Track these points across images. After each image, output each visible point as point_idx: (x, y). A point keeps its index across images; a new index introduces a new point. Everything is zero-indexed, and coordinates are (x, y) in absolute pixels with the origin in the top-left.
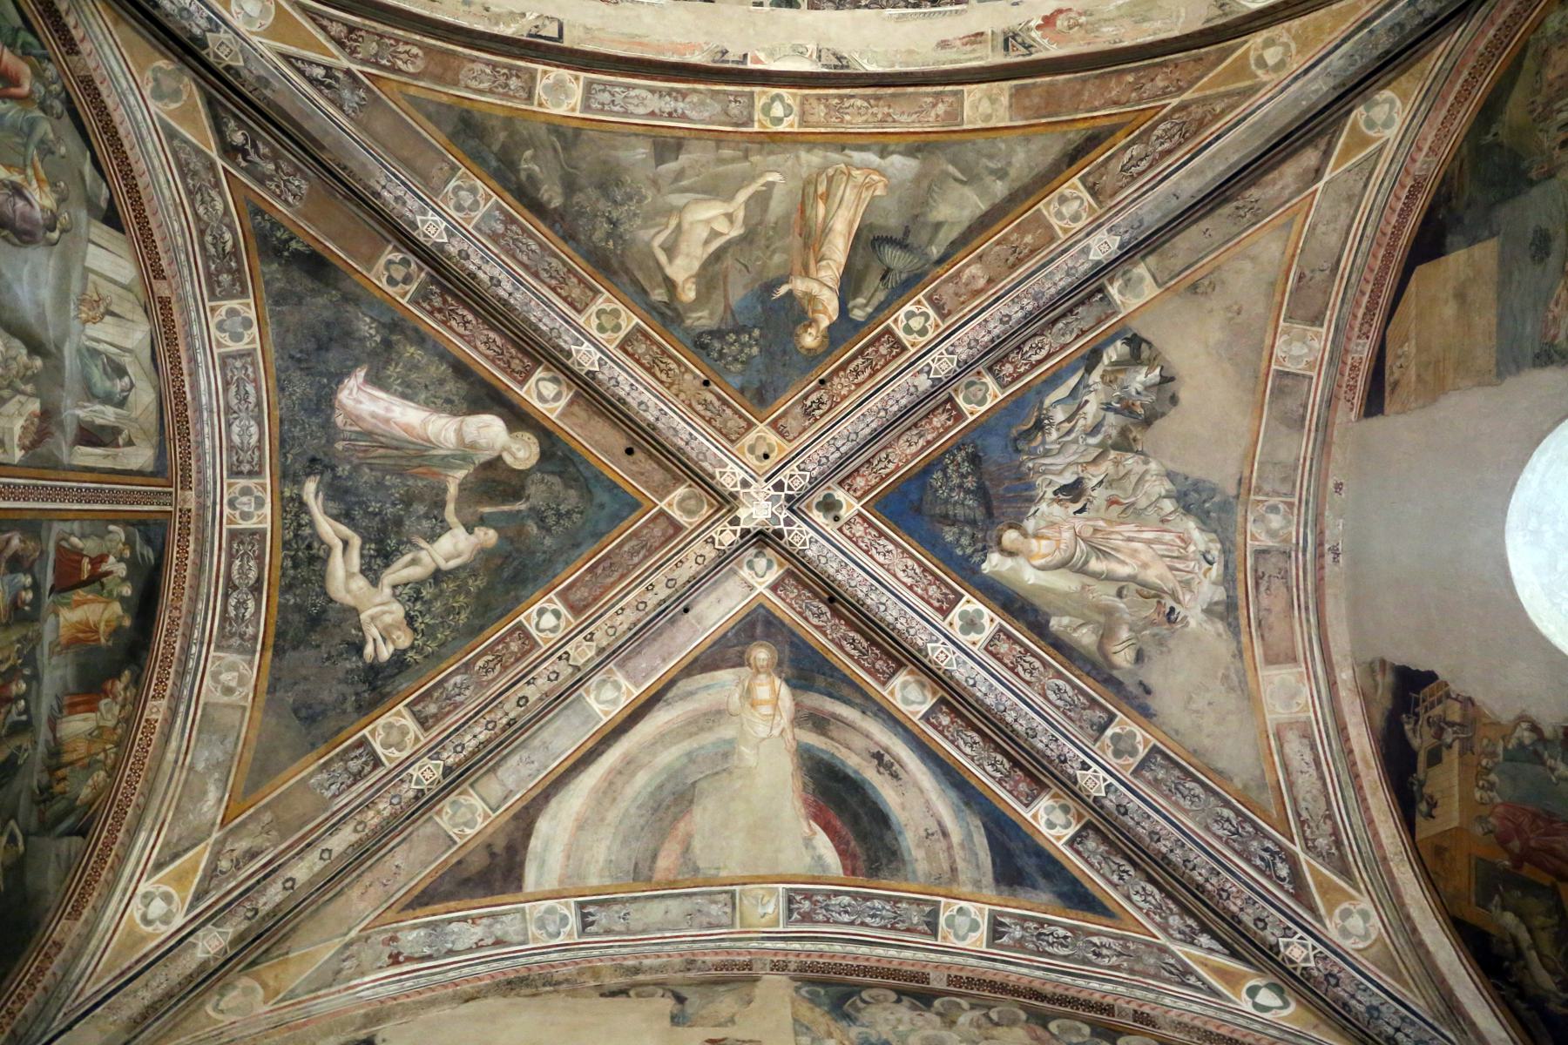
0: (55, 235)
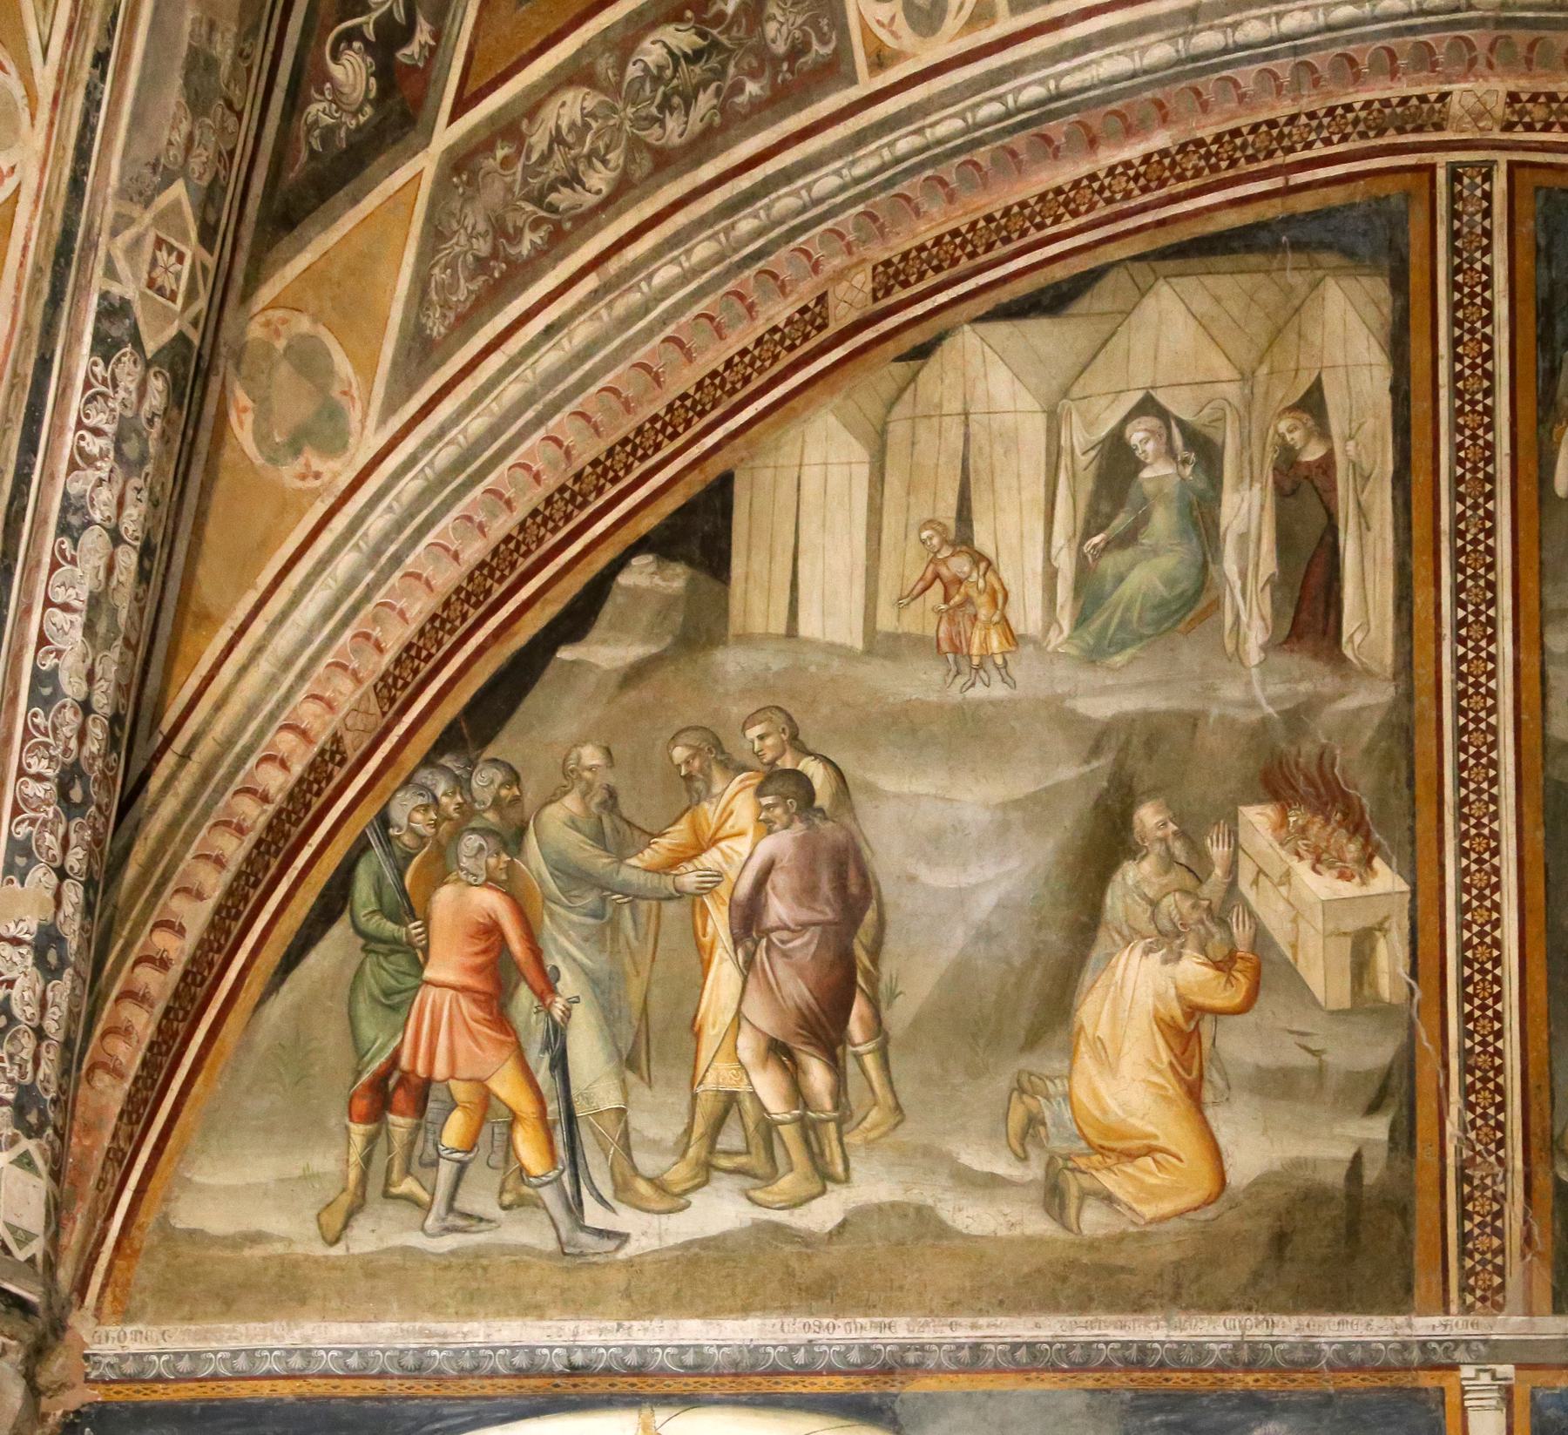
0: (815, 771)
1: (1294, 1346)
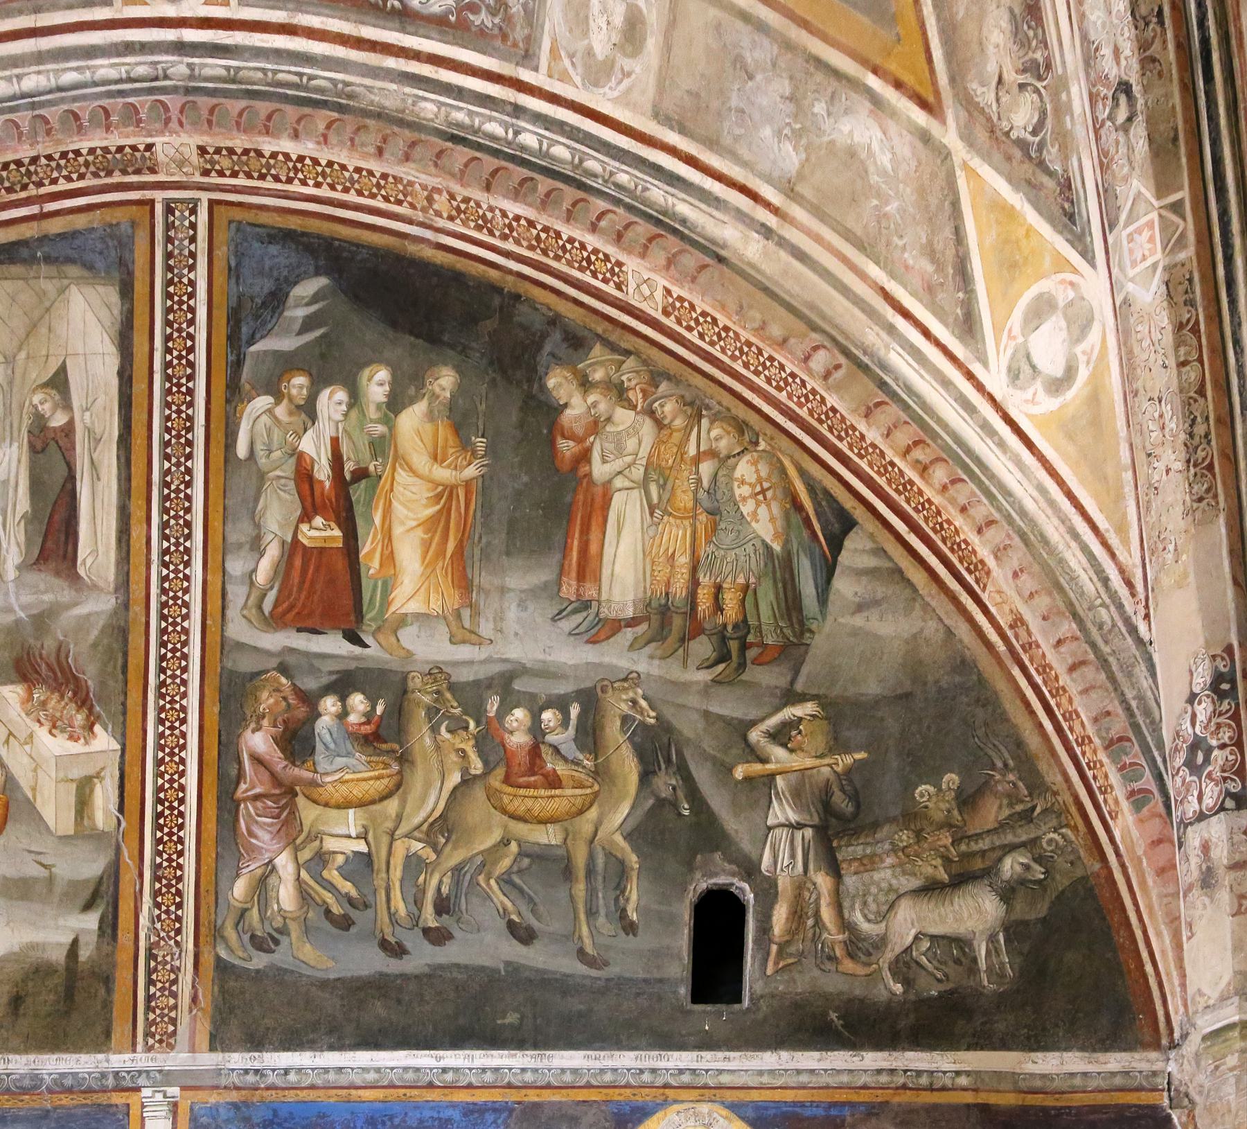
1: (23, 1076)
